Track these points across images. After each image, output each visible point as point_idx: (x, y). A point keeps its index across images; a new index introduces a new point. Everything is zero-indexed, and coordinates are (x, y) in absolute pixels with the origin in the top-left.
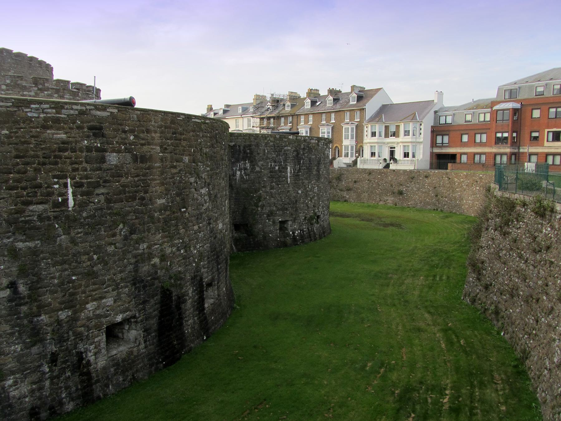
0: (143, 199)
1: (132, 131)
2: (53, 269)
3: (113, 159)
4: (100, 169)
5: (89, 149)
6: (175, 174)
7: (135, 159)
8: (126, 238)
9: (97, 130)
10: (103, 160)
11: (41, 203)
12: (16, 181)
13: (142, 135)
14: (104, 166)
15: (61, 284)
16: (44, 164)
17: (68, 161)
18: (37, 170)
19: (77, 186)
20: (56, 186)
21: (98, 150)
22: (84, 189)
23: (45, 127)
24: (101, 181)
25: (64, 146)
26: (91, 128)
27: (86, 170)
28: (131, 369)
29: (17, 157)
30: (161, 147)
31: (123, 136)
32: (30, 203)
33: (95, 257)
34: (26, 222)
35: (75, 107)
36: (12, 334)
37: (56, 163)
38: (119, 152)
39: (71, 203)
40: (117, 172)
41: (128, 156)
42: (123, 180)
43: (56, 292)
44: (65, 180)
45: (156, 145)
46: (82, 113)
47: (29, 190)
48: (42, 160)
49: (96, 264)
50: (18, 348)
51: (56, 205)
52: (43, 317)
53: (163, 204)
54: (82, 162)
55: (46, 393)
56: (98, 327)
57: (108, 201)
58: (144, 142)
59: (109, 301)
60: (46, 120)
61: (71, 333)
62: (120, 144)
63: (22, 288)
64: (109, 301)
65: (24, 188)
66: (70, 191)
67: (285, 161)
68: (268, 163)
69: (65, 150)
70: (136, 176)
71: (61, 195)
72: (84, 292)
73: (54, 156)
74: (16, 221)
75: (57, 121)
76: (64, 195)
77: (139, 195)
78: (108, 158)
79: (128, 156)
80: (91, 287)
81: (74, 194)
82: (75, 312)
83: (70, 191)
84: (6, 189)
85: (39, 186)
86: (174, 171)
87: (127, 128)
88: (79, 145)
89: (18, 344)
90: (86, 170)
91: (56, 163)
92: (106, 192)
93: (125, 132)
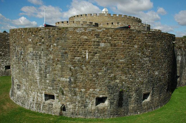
0: (114, 59)
1: (111, 36)
2: (80, 76)
3: (102, 45)
4: (98, 48)
5: (94, 42)
6: (130, 51)
7: (112, 45)
8: (105, 71)
10: (99, 45)
11: (78, 57)
12: (73, 50)
13: (115, 37)
14: (99, 47)
15: (82, 81)
16: (80, 45)
17: (87, 45)
19: (90, 52)
20: (83, 52)
21: (97, 42)
22: (92, 54)
24: (98, 52)
25: (87, 40)
26: (95, 35)
27: (92, 48)
28: (103, 113)
29: (73, 43)
30: (124, 41)
31: (107, 37)
32: (75, 56)
33: (94, 75)
34: (75, 62)
35: (90, 29)
36: (69, 91)
37: (83, 45)
38: (105, 43)
39: (87, 57)
40: (104, 49)
41: (109, 44)
42: (106, 52)
43: (81, 83)
44: (86, 51)
45: (121, 41)
47: (76, 53)
48: (79, 44)
49: (94, 78)
50: (70, 95)
51: (83, 58)
52: (77, 89)
53: (123, 62)
54: (91, 45)
55: (76, 110)
56: (93, 97)
57: (100, 58)
58: (115, 40)
59: (98, 90)
60: (82, 33)
61: (84, 96)
62: (105, 40)
63: (72, 80)
64: (98, 90)
65: (75, 52)
66: (87, 54)
69: (87, 42)
70: (111, 51)
71: (84, 55)
72: (90, 85)
73: (82, 44)
74: (72, 61)
75: (85, 33)
77: (112, 58)
78: (100, 45)
80: (92, 84)
81: (88, 55)
82: (86, 90)
83: (87, 54)
84: (70, 52)
85: (79, 52)
86: (129, 50)
87: (109, 35)
88: (91, 40)
89: (70, 94)
90: (92, 48)
91: (83, 45)
92: (99, 55)
93: (108, 36)
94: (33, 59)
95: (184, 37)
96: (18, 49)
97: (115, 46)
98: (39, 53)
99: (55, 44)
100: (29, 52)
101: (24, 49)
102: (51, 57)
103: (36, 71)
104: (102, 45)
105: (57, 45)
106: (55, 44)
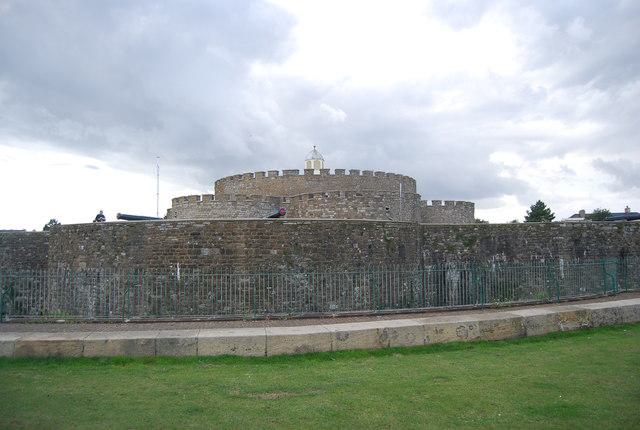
3: (206, 252)
5: (191, 246)
7: (223, 252)
9: (196, 235)
10: (199, 252)
12: (154, 263)
18: (163, 258)
19: (181, 267)
21: (196, 246)
23: (167, 235)
25: (176, 245)
41: (218, 251)
46: (188, 226)
60: (168, 231)
67: (555, 252)
68: (529, 255)
71: (173, 271)
73: (170, 251)
75: (174, 231)
76: (175, 272)
79: (218, 251)
86: (257, 259)
94: (85, 284)
95: (629, 217)
96: (61, 265)
97: (229, 252)
98: (97, 270)
99: (124, 254)
100: (79, 269)
101: (71, 266)
102: (117, 277)
103: (91, 307)
104: (206, 252)
105: (127, 256)
106: (124, 254)
